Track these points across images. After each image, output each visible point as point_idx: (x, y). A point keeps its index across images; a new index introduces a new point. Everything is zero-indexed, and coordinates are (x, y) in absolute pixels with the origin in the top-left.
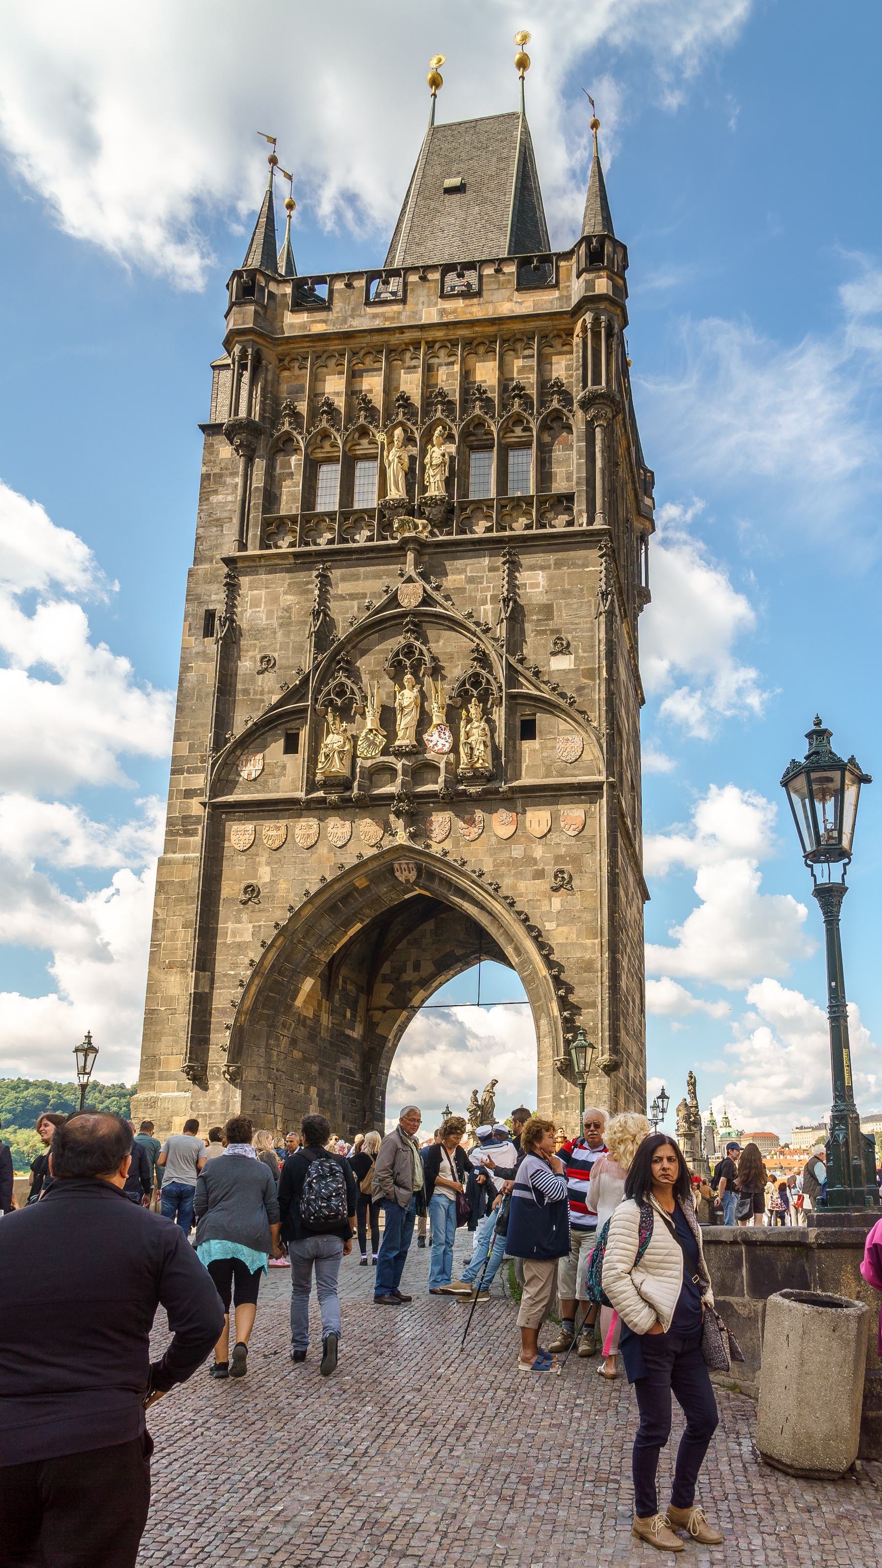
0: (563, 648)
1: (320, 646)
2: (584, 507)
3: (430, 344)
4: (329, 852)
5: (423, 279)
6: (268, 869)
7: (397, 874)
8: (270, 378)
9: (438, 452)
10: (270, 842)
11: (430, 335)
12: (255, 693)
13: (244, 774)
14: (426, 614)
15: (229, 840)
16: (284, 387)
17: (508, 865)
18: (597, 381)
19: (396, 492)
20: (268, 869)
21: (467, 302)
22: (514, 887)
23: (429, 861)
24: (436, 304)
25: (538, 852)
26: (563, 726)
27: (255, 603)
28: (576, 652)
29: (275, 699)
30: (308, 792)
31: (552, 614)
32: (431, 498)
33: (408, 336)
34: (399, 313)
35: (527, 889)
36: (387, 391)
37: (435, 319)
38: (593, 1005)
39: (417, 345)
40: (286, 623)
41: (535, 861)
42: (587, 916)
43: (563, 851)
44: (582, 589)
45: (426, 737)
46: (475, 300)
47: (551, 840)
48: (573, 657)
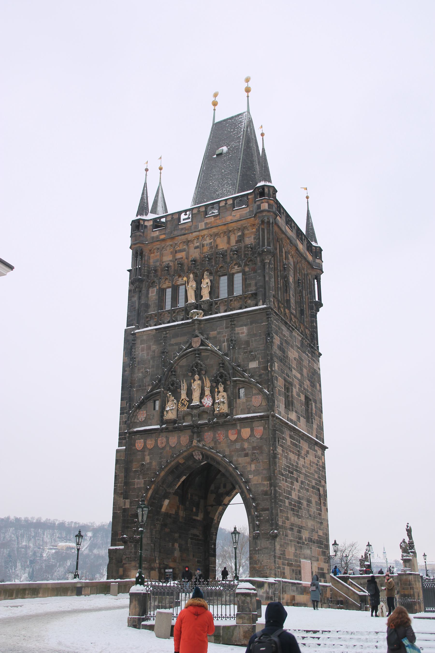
0: (254, 359)
2: (261, 298)
3: (203, 237)
4: (170, 449)
5: (199, 211)
7: (195, 457)
8: (146, 259)
9: (206, 282)
10: (149, 446)
13: (140, 419)
14: (202, 349)
15: (135, 446)
16: (151, 261)
18: (263, 245)
19: (192, 300)
21: (215, 218)
22: (237, 461)
23: (205, 451)
24: (204, 221)
25: (246, 445)
26: (254, 392)
27: (143, 350)
28: (259, 360)
29: (150, 388)
30: (161, 426)
32: (203, 301)
34: (191, 226)
35: (242, 460)
36: (187, 258)
37: (204, 227)
38: (267, 509)
40: (153, 358)
41: (244, 449)
42: (265, 472)
43: (255, 445)
45: (203, 401)
46: (218, 217)
47: (251, 440)
48: (257, 361)
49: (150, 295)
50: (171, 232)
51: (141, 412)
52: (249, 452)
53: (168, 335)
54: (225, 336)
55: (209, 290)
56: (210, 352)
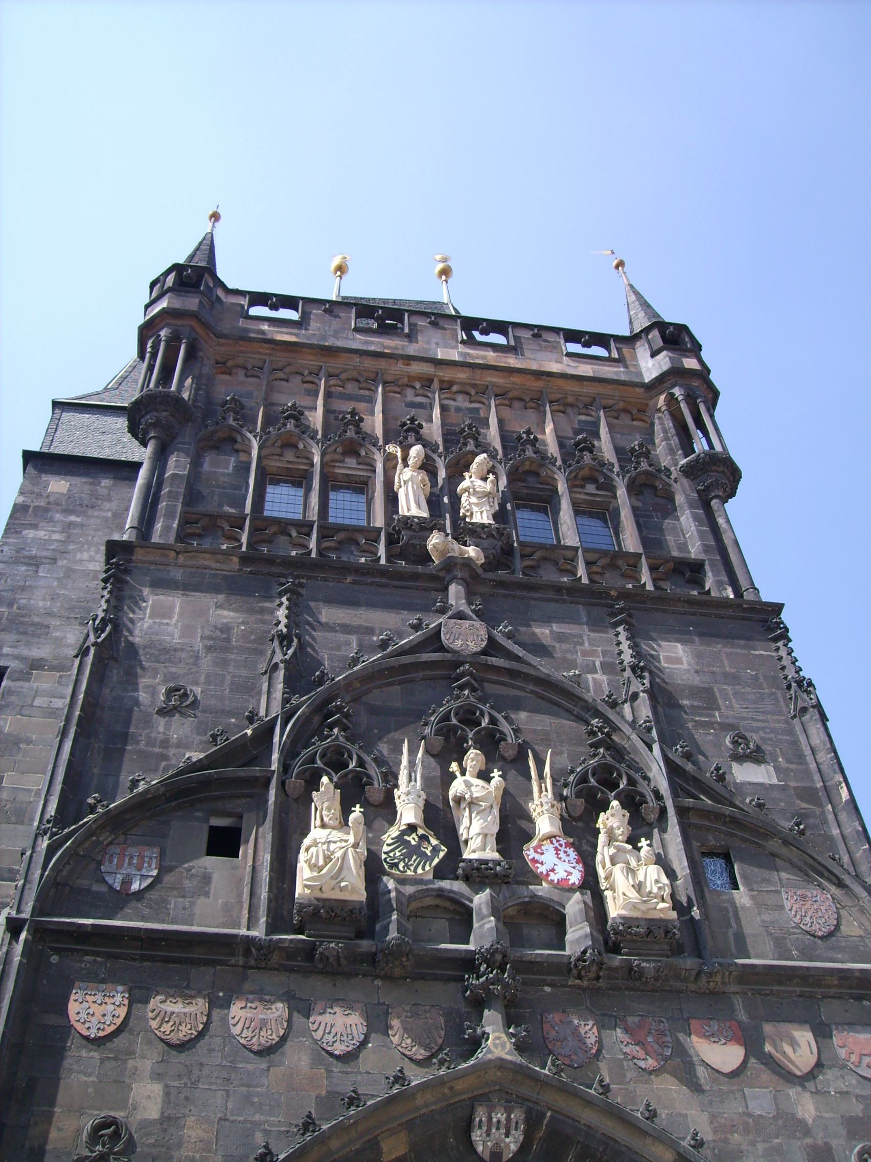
1: (293, 685)
6: (157, 1089)
7: (477, 1136)
11: (447, 374)
12: (150, 742)
15: (64, 1012)
17: (747, 1131)
20: (157, 1089)
25: (806, 1107)
27: (162, 612)
28: (775, 761)
30: (272, 928)
31: (715, 701)
32: (483, 526)
33: (417, 368)
34: (403, 347)
39: (427, 382)
43: (857, 1109)
44: (756, 678)
49: (206, 467)
50: (324, 338)
51: (132, 850)
52: (834, 1143)
53: (300, 590)
54: (594, 653)
55: (497, 508)
56: (531, 687)
